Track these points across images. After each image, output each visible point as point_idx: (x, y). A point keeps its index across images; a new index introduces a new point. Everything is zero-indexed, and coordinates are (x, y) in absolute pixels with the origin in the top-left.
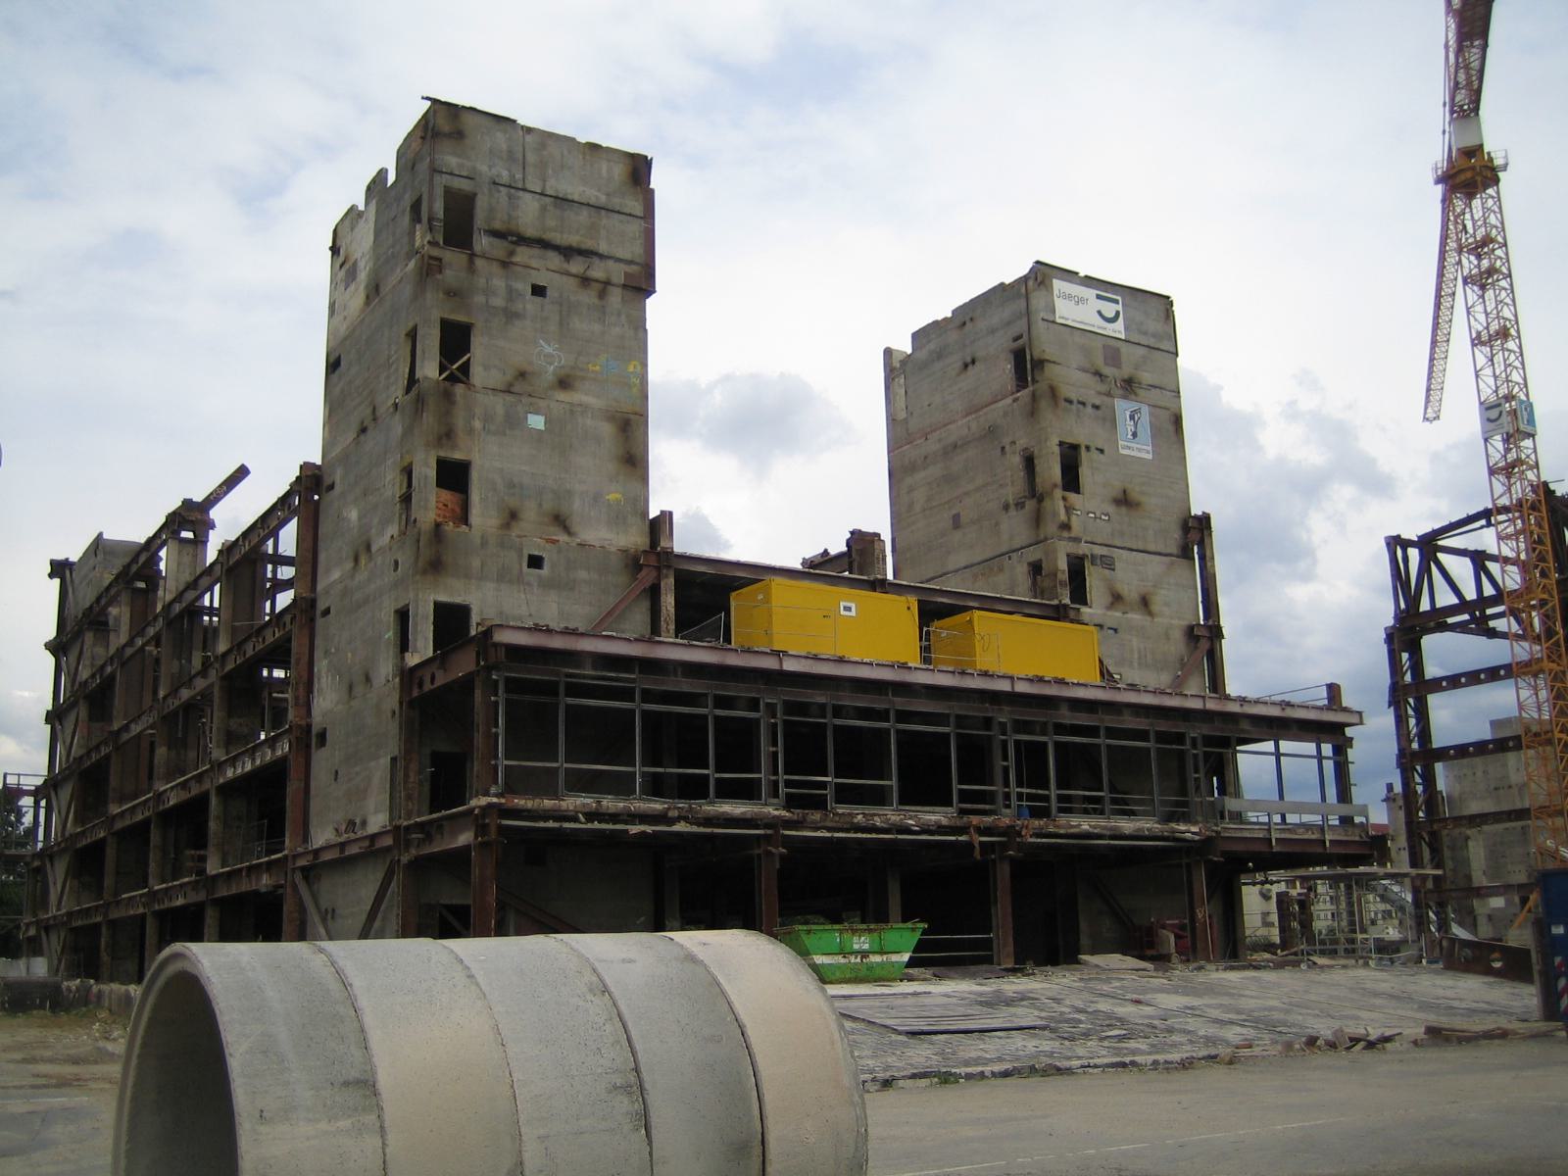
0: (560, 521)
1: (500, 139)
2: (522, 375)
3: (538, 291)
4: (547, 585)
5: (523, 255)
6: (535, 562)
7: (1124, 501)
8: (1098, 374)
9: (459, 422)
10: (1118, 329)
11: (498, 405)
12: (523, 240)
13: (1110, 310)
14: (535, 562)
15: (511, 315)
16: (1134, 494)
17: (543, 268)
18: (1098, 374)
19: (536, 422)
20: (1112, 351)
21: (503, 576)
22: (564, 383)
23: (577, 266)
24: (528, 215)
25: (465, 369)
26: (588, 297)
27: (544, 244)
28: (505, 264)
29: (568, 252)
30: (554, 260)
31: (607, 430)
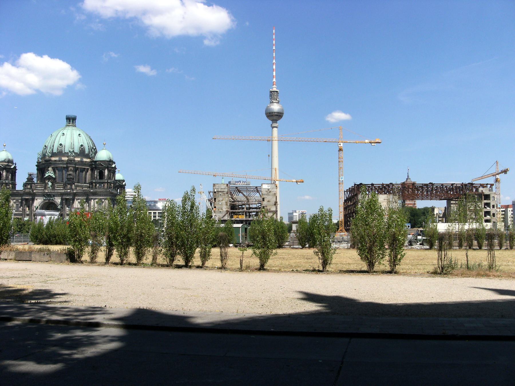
0: (222, 209)
1: (218, 185)
2: (219, 201)
3: (220, 195)
4: (221, 213)
5: (219, 193)
6: (220, 212)
7: (269, 201)
8: (267, 192)
9: (215, 204)
10: (269, 187)
11: (218, 203)
12: (219, 192)
13: (269, 186)
14: (220, 212)
15: (219, 197)
16: (270, 200)
17: (220, 193)
18: (267, 192)
19: (220, 203)
20: (268, 190)
21: (218, 213)
22: (222, 201)
23: (223, 193)
24: (220, 190)
25: (216, 201)
26: (224, 194)
27: (221, 192)
28: (218, 194)
29: (222, 192)
30: (221, 192)
31: (225, 203)
